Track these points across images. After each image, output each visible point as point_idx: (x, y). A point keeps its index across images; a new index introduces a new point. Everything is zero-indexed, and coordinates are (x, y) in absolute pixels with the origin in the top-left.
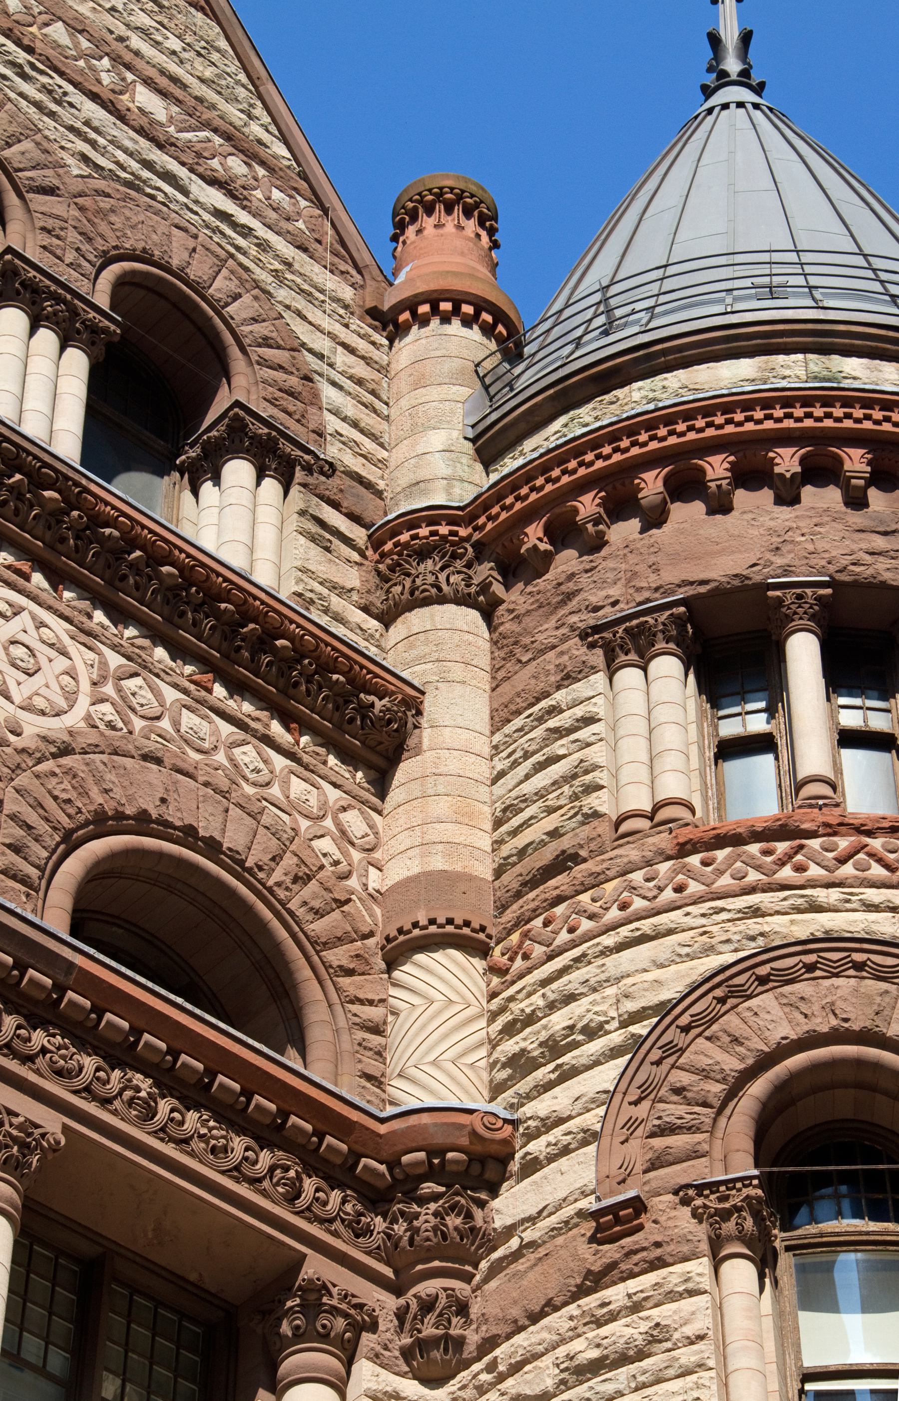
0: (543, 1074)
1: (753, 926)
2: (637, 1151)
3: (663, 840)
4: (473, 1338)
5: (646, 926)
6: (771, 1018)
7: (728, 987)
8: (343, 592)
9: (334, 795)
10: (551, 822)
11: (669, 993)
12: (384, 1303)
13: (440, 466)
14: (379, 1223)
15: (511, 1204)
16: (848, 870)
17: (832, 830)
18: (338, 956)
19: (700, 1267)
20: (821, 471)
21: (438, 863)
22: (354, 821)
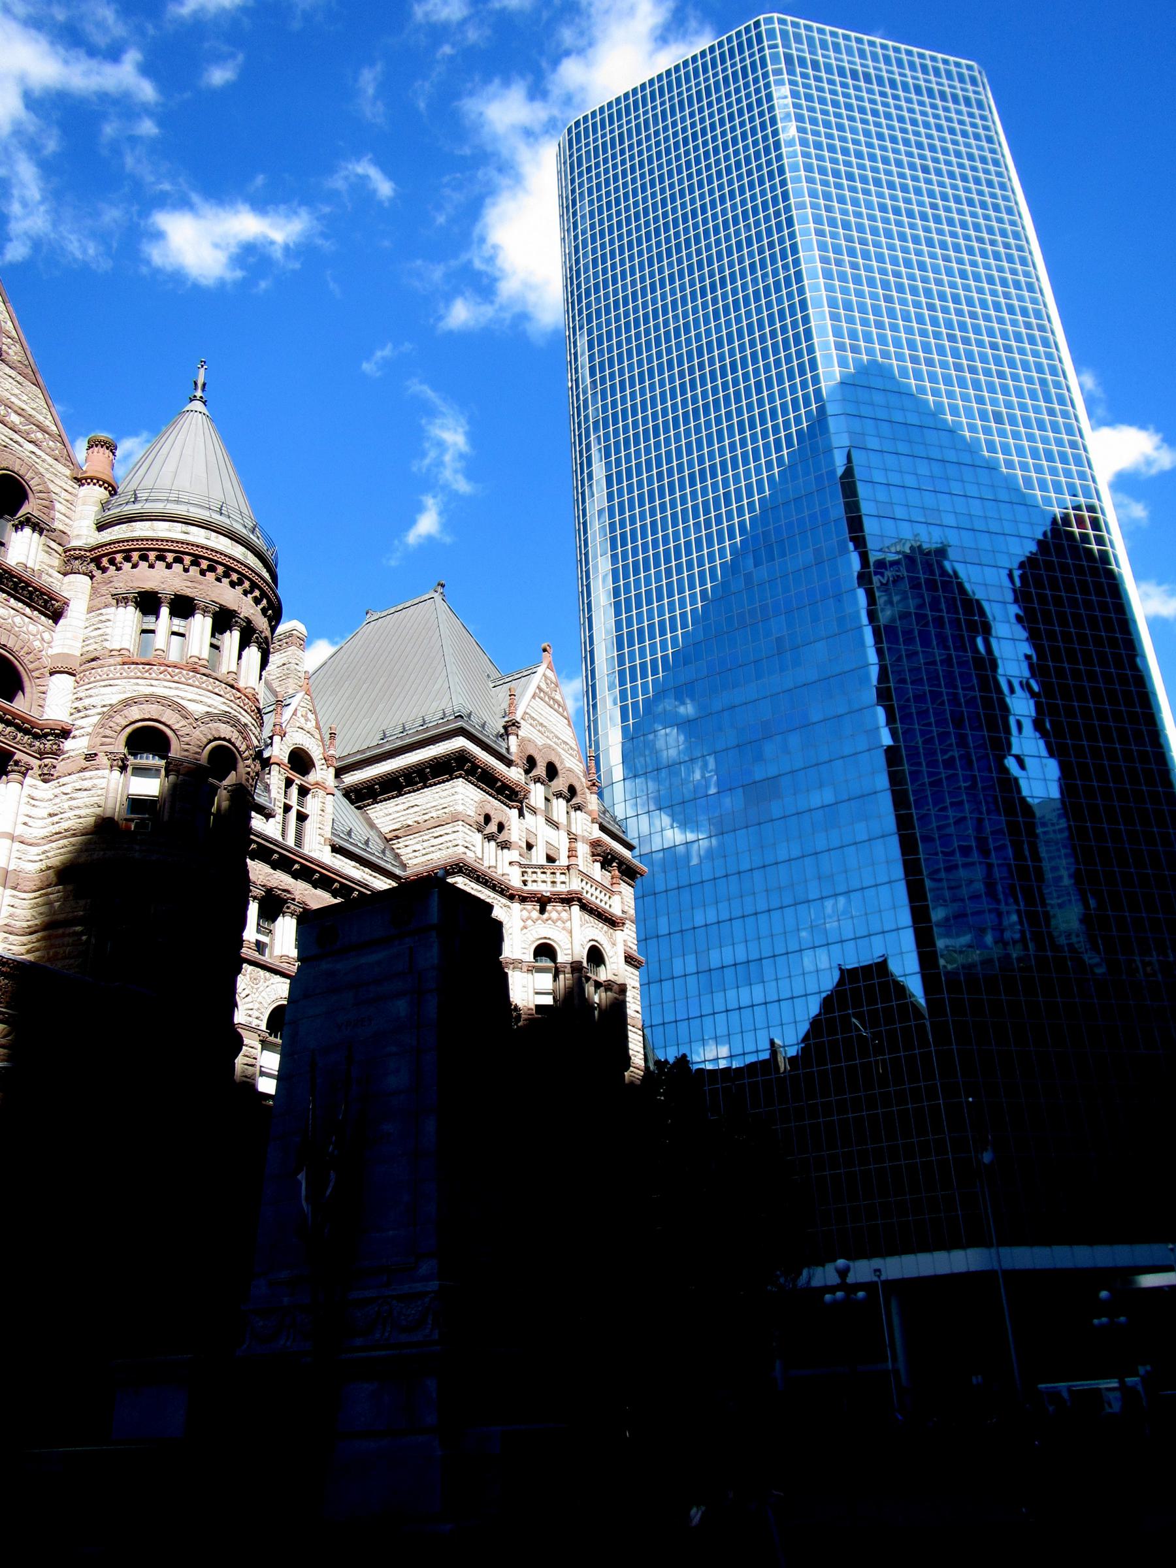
0: (81, 714)
1: (136, 688)
2: (99, 740)
3: (119, 659)
4: (56, 775)
5: (111, 682)
6: (135, 713)
7: (128, 703)
8: (52, 567)
9: (41, 628)
10: (95, 646)
11: (114, 702)
12: (35, 763)
13: (84, 532)
14: (38, 744)
15: (68, 745)
16: (162, 676)
17: (160, 665)
18: (35, 674)
19: (107, 771)
20: (178, 560)
21: (66, 651)
22: (46, 636)
